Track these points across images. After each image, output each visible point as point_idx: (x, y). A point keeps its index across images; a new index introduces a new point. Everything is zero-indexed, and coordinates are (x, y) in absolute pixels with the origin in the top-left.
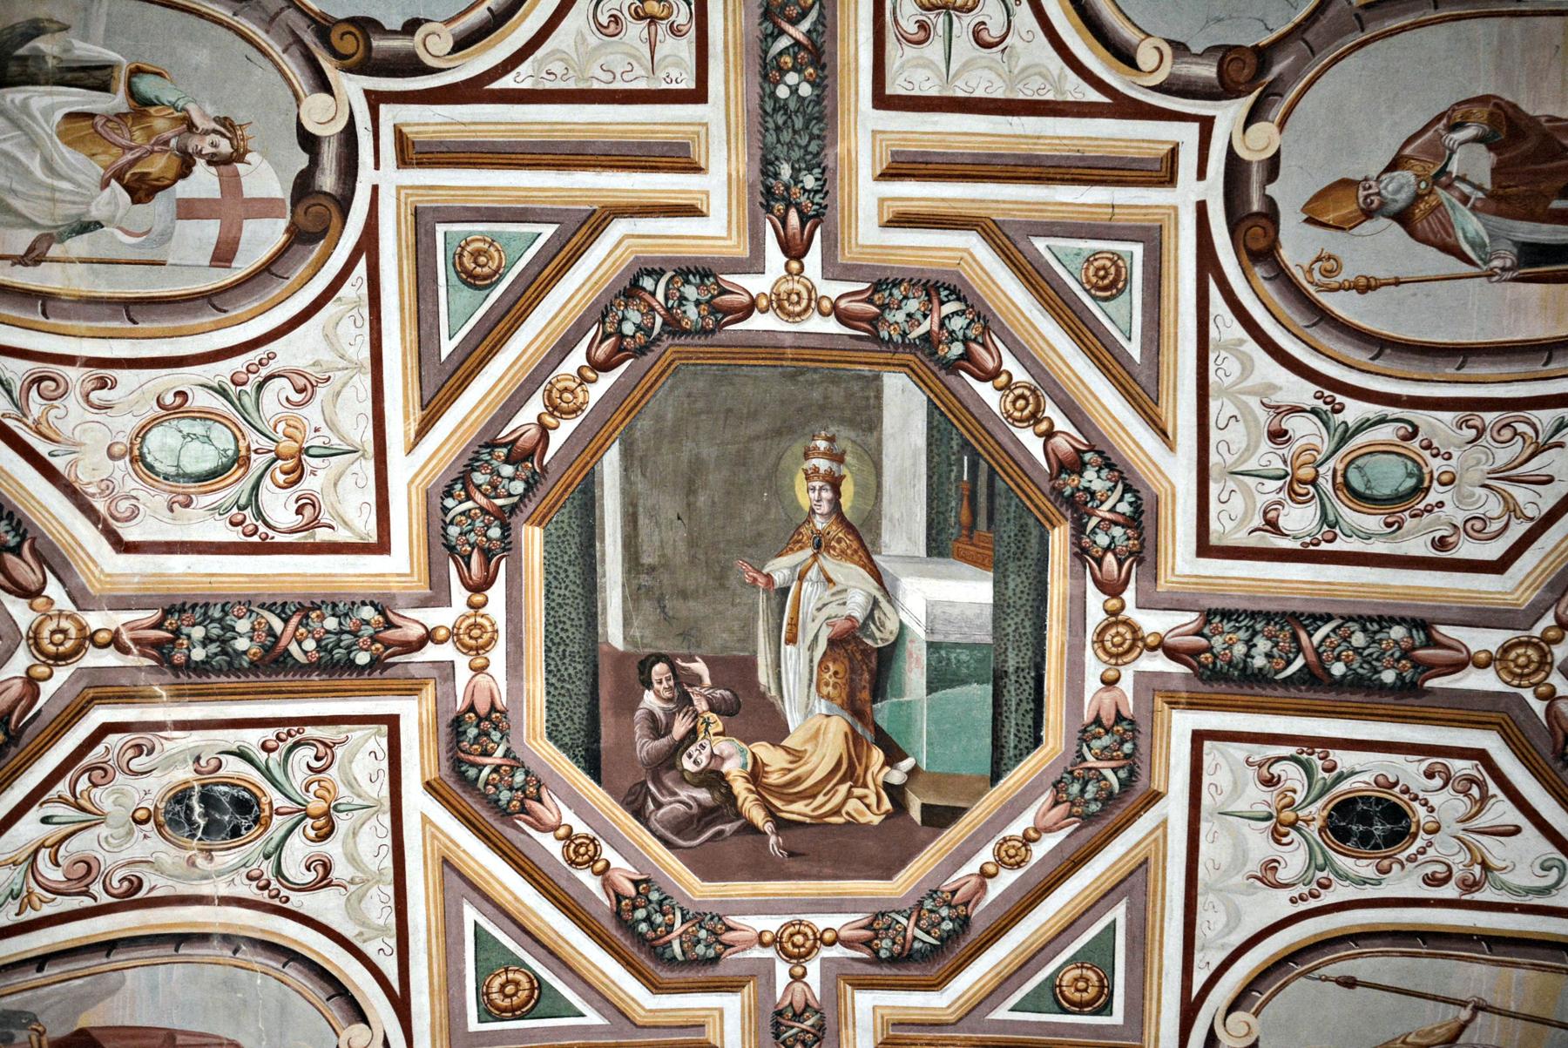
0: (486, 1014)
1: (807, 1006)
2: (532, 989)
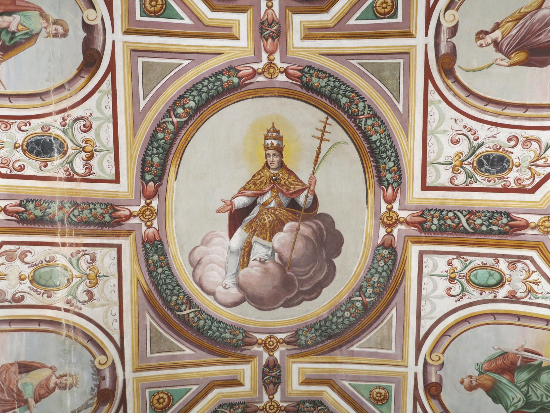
0: (145, 12)
1: (273, 20)
2: (163, 4)
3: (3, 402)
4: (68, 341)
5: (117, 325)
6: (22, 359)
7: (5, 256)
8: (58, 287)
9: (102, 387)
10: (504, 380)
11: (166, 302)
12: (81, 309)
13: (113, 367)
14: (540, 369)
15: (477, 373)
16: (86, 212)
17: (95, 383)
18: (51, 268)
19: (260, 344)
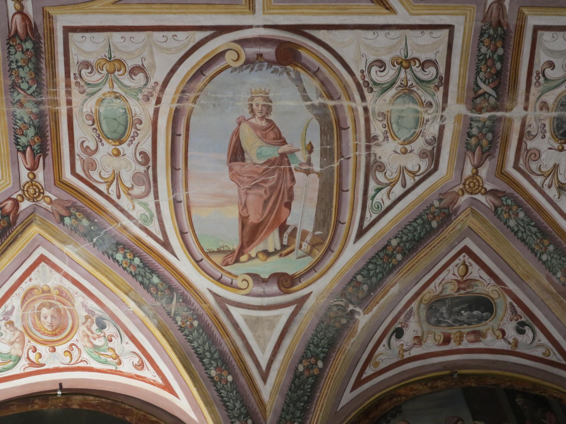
3: (281, 182)
4: (201, 100)
5: (181, 35)
6: (224, 157)
7: (90, 172)
8: (127, 111)
9: (274, 58)
12: (156, 83)
13: (243, 42)
16: (22, 73)
17: (265, 68)
18: (102, 118)
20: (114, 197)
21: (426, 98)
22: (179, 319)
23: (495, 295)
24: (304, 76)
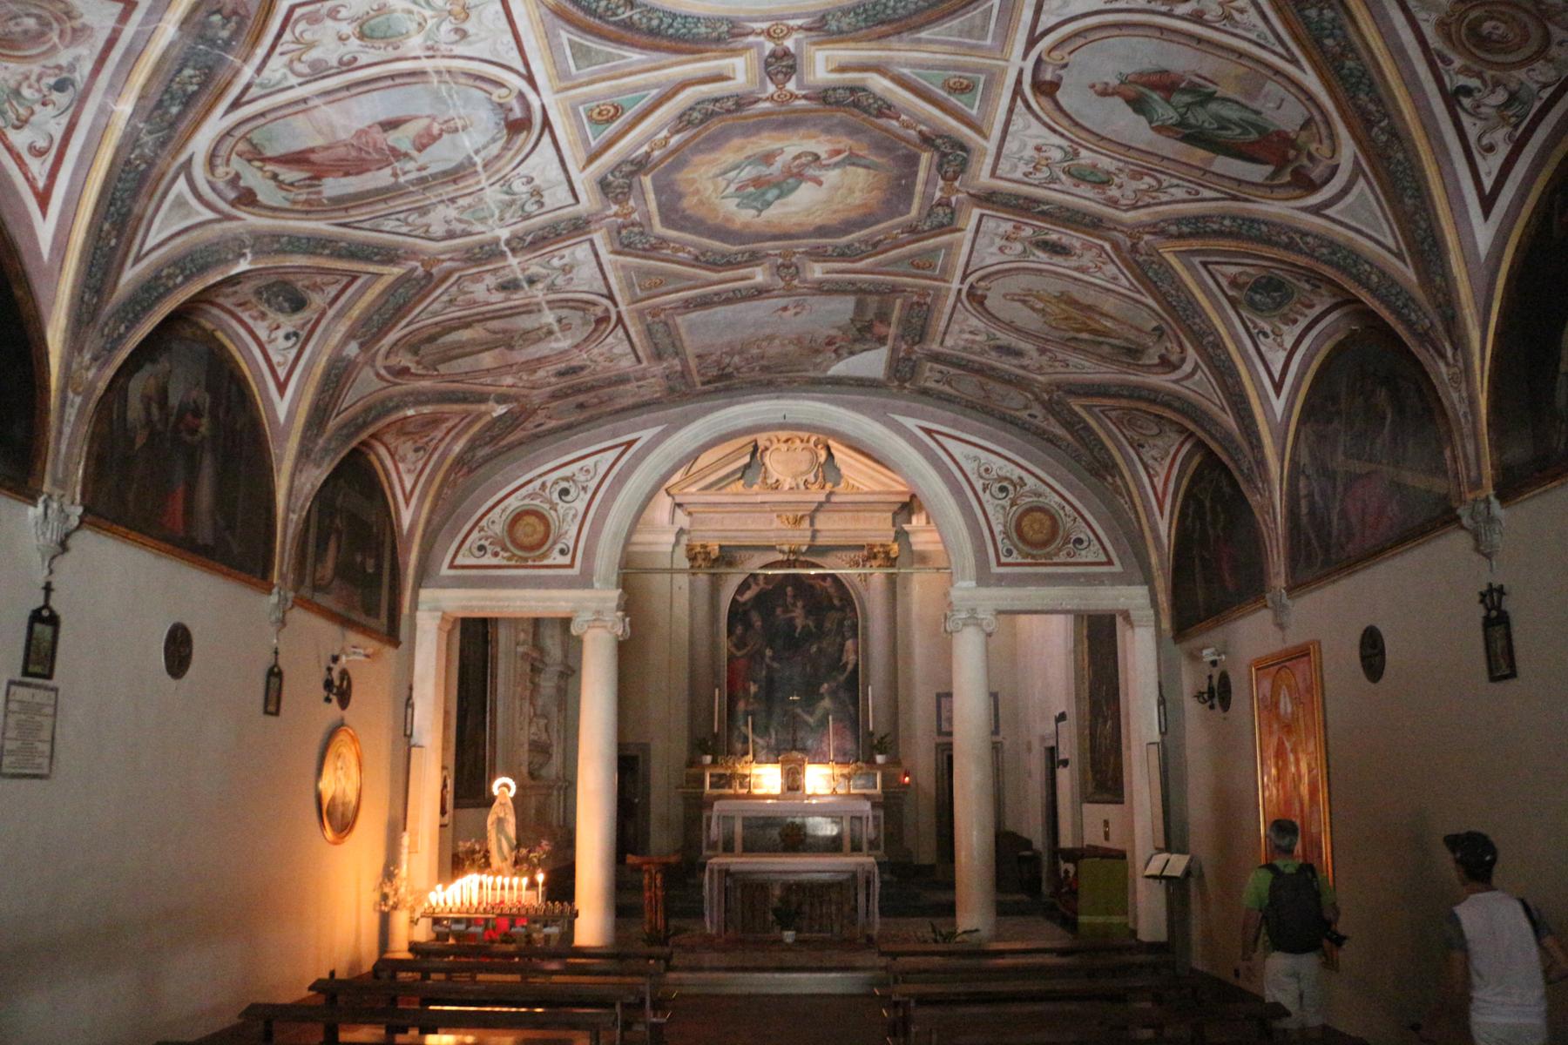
4: (443, 87)
5: (515, 53)
6: (382, 117)
8: (407, 35)
10: (1155, 96)
11: (592, 13)
13: (521, 96)
14: (1211, 97)
15: (1117, 82)
19: (759, 34)
20: (279, 49)
21: (507, 216)
22: (137, 151)
23: (314, 306)
24: (500, 143)
